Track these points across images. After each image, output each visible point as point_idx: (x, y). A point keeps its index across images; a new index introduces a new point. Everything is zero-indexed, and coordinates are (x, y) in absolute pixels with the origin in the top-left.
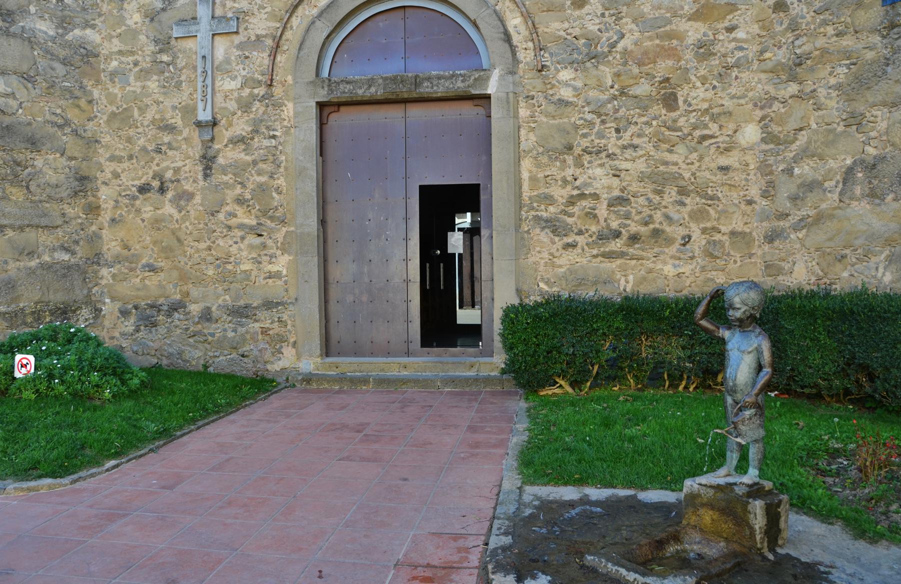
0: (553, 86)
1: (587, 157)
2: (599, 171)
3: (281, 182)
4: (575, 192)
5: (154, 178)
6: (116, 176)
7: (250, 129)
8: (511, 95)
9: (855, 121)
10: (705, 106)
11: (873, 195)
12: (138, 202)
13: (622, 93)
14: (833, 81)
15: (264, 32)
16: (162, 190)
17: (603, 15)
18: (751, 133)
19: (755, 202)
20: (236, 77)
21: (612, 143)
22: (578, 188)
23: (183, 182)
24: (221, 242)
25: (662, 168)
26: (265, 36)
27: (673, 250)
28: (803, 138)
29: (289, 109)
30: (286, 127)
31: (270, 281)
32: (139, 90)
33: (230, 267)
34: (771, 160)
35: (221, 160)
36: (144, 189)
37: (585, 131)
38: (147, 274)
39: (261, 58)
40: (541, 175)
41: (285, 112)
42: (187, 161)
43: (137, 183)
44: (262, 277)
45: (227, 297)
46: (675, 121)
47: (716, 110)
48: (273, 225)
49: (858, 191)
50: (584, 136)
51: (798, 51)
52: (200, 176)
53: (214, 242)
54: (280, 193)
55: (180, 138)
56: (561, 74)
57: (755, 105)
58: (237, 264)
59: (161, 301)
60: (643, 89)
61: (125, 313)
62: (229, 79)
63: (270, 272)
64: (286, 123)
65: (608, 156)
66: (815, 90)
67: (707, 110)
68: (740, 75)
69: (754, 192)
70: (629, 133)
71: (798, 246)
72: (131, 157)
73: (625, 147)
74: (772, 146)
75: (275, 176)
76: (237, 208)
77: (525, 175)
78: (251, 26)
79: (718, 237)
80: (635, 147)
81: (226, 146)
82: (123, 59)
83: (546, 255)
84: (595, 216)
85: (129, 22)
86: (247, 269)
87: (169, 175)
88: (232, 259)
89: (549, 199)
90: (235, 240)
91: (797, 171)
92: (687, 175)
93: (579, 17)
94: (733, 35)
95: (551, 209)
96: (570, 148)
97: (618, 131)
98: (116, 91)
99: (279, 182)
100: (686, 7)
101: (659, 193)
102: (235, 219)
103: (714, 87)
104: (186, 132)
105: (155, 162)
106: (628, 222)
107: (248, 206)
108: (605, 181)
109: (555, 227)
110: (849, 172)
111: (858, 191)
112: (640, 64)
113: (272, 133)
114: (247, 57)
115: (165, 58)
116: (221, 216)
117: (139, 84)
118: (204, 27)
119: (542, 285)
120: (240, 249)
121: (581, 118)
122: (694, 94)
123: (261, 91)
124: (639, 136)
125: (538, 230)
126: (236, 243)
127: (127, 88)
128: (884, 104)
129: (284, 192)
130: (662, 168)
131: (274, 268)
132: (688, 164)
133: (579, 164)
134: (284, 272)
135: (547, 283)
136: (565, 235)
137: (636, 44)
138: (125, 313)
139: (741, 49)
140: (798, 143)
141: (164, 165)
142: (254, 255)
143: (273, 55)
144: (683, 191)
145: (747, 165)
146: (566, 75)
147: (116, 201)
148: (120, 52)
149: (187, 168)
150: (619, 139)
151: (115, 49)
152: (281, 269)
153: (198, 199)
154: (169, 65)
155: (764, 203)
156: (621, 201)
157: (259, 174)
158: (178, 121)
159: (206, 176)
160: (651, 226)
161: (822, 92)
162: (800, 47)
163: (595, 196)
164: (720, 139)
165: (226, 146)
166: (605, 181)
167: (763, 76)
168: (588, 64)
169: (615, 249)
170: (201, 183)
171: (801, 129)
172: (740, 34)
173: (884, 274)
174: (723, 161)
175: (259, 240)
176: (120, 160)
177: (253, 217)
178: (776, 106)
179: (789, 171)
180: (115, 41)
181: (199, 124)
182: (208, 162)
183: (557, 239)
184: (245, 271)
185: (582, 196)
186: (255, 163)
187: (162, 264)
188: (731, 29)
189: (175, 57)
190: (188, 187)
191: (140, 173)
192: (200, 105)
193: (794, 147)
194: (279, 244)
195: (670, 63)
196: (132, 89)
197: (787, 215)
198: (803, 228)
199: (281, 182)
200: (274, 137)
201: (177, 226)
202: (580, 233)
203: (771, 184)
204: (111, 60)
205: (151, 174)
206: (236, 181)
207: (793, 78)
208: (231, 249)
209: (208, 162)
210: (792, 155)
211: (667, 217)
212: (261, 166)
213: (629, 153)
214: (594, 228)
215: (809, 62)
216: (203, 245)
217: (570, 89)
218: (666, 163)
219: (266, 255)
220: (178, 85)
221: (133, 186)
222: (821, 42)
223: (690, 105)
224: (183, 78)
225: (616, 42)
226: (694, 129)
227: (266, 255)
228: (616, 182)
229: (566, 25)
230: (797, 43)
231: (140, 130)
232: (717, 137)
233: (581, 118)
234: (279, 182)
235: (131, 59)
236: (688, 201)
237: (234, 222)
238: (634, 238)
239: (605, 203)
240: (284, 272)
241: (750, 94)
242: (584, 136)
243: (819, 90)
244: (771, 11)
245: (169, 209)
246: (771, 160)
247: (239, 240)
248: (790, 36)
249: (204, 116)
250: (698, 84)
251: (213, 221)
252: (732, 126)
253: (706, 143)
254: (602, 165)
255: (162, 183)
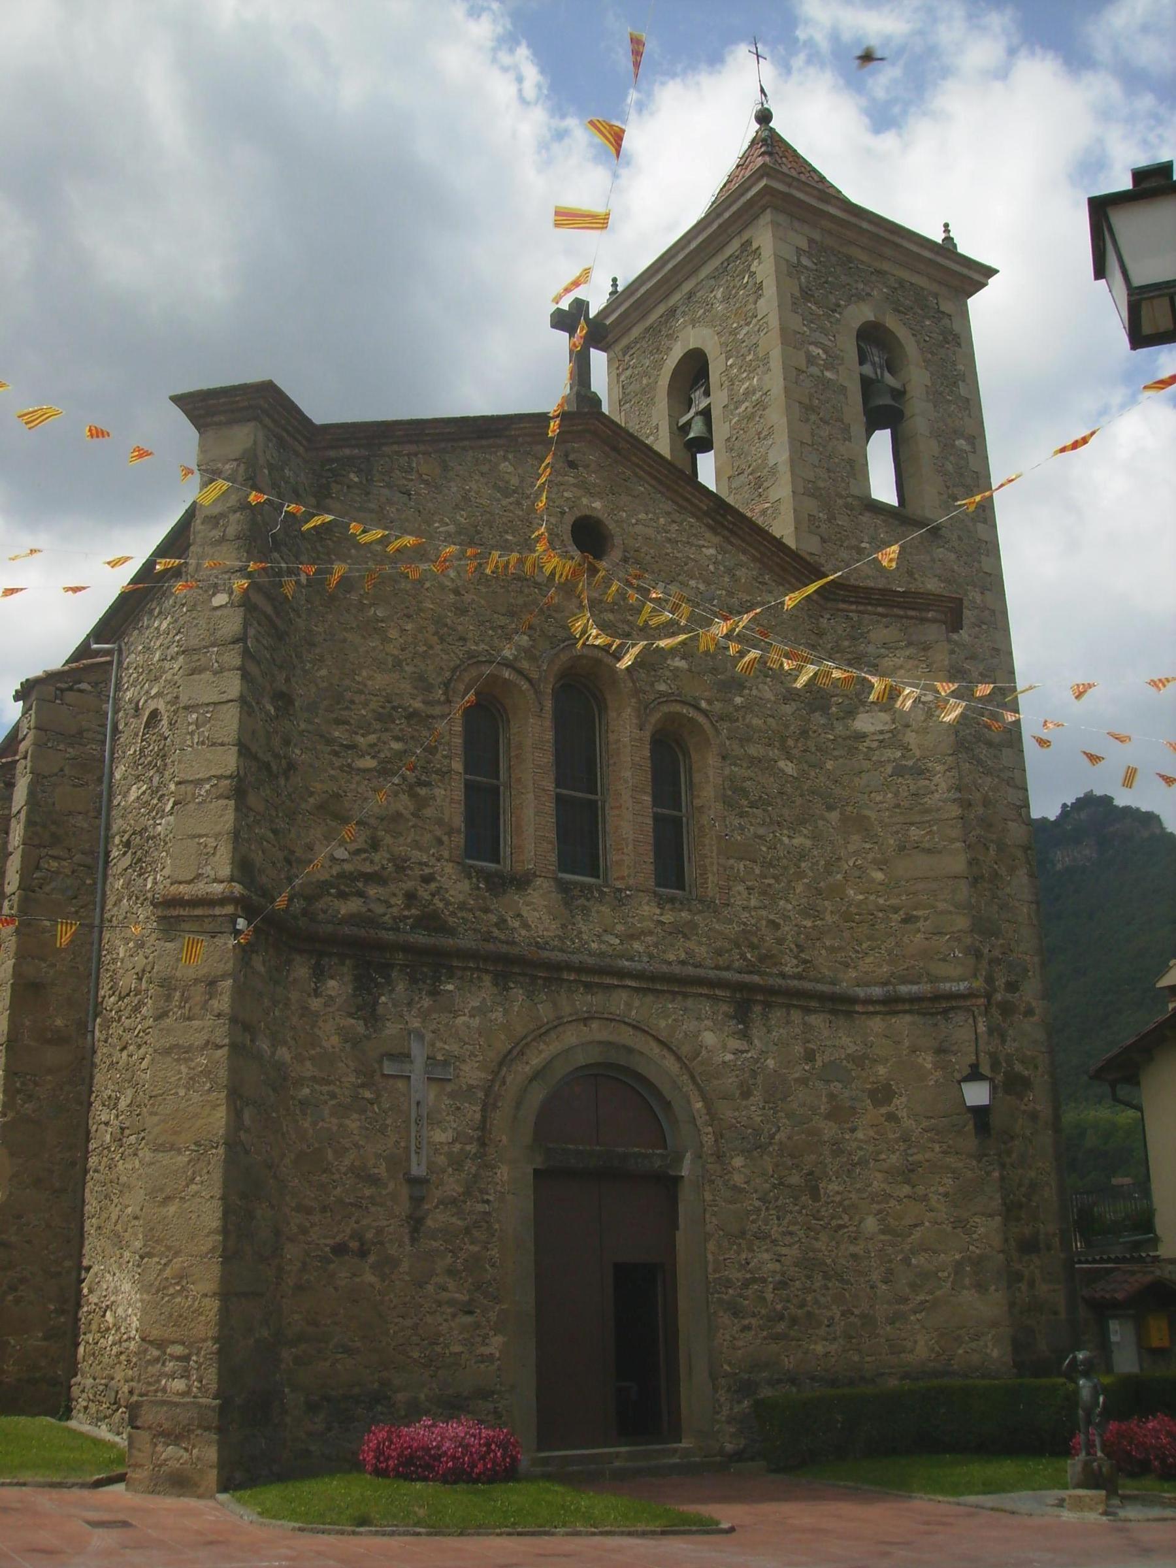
0: (730, 1172)
1: (757, 1242)
2: (766, 1256)
3: (494, 1252)
4: (748, 1276)
5: (351, 1237)
6: (304, 1231)
7: (461, 1190)
8: (700, 1179)
9: (960, 1224)
10: (838, 1198)
11: (981, 1287)
12: (332, 1266)
13: (781, 1184)
14: (941, 1190)
15: (475, 1083)
16: (363, 1254)
17: (764, 1108)
18: (871, 1224)
19: (876, 1287)
20: (446, 1129)
21: (775, 1232)
22: (751, 1272)
23: (387, 1245)
24: (429, 1319)
25: (811, 1254)
26: (476, 1087)
27: (822, 1331)
28: (917, 1234)
29: (503, 1172)
30: (500, 1192)
31: (482, 1366)
32: (335, 1128)
33: (438, 1349)
34: (890, 1250)
35: (429, 1223)
36: (340, 1250)
37: (754, 1217)
38: (340, 1356)
39: (473, 1112)
40: (721, 1258)
41: (499, 1174)
42: (392, 1221)
43: (330, 1242)
44: (473, 1362)
45: (434, 1386)
46: (818, 1211)
47: (846, 1203)
48: (485, 1302)
49: (967, 1281)
50: (753, 1222)
51: (910, 1159)
52: (406, 1240)
53: (421, 1320)
54: (493, 1266)
55: (384, 1192)
56: (734, 1160)
57: (873, 1199)
58: (447, 1346)
59: (356, 1390)
60: (795, 1179)
61: (312, 1408)
62: (438, 1130)
63: (482, 1355)
64: (499, 1188)
65: (772, 1242)
66: (926, 1195)
67: (840, 1203)
68: (862, 1172)
69: (875, 1276)
70: (786, 1221)
71: (917, 1326)
72: (324, 1209)
73: (784, 1234)
74: (887, 1237)
75: (489, 1246)
76: (448, 1280)
77: (710, 1257)
78: (462, 1073)
79: (852, 1319)
80: (791, 1233)
81: (437, 1207)
82: (317, 1087)
83: (728, 1337)
84: (764, 1299)
85: (324, 1043)
86: (457, 1351)
87: (369, 1235)
88: (442, 1339)
89: (728, 1284)
90: (445, 1316)
91: (914, 1261)
92: (829, 1261)
93: (746, 1107)
94: (855, 1135)
95: (731, 1291)
96: (743, 1233)
97: (778, 1218)
98: (306, 1125)
99: (493, 1253)
100: (822, 1107)
101: (809, 1277)
102: (444, 1293)
103: (845, 1182)
104: (391, 1186)
105: (354, 1219)
106: (788, 1305)
107: (461, 1278)
108: (772, 1266)
109: (736, 1312)
110: (958, 1267)
111: (967, 1281)
112: (792, 1156)
113: (486, 1197)
114: (458, 1108)
115: (368, 1094)
116: (430, 1288)
117: (335, 1121)
118: (417, 1069)
119: (726, 1367)
120: (451, 1329)
121: (750, 1205)
122: (830, 1187)
123: (472, 1148)
124: (795, 1224)
125: (721, 1314)
126: (446, 1320)
127: (321, 1124)
128: (983, 1214)
129: (498, 1264)
130: (811, 1254)
131: (486, 1350)
132: (830, 1251)
133: (751, 1250)
134: (497, 1355)
135: (730, 1364)
136: (743, 1318)
137: (789, 1138)
138: (312, 1408)
139: (861, 1149)
140: (913, 1237)
141: (364, 1222)
142: (466, 1336)
143: (487, 1108)
144: (826, 1276)
145: (869, 1252)
146: (738, 1162)
147: (304, 1263)
148: (313, 1078)
149: (391, 1229)
150: (779, 1226)
151: (308, 1074)
152: (493, 1352)
153: (405, 1266)
154: (372, 1104)
155: (884, 1287)
156: (783, 1285)
157: (472, 1243)
158: (382, 1170)
159: (413, 1240)
160: (806, 1309)
161: (934, 1198)
162: (912, 1155)
163: (764, 1280)
164: (851, 1229)
165: (437, 1207)
166: (772, 1266)
167: (878, 1175)
168: (755, 1153)
169: (780, 1330)
170: (408, 1248)
171: (916, 1226)
172: (860, 1135)
173: (992, 1350)
174: (853, 1249)
175: (469, 1319)
176: (309, 1211)
177: (465, 1292)
178: (892, 1203)
179: (906, 1261)
180: (308, 1064)
181: (413, 1181)
182: (416, 1223)
183: (736, 1321)
184: (456, 1354)
185: (754, 1280)
186: (467, 1231)
187: (359, 1344)
188: (853, 1130)
189: (379, 1096)
190: (393, 1250)
191: (335, 1230)
192: (414, 1158)
193: (909, 1240)
194: (492, 1323)
195: (813, 1157)
196: (326, 1125)
197: (907, 1299)
198: (921, 1311)
199: (494, 1252)
200: (487, 1202)
201: (378, 1298)
202: (754, 1315)
203: (890, 1272)
204: (303, 1085)
205: (348, 1231)
206: (446, 1248)
207: (908, 1182)
208: (441, 1328)
209: (416, 1223)
210: (908, 1247)
211: (816, 1302)
212: (476, 1233)
213: (788, 1240)
214: (763, 1312)
215: (920, 1169)
216: (409, 1322)
217: (742, 1176)
218: (814, 1251)
219: (479, 1335)
220: (383, 1131)
221: (326, 1245)
222: (928, 1155)
223: (829, 1197)
224: (389, 1121)
225: (775, 1134)
226: (832, 1219)
227: (479, 1335)
228: (778, 1266)
229: (736, 1114)
230: (909, 1152)
231: (336, 1177)
232: (847, 1227)
233: (750, 1205)
234: (493, 1253)
235: (325, 1089)
236: (830, 1285)
237: (445, 1295)
238: (794, 1321)
239: (771, 1286)
240: (497, 1355)
241: (869, 1189)
242: (753, 1222)
243: (930, 1195)
244: (883, 1119)
245: (369, 1278)
246: (890, 1250)
247: (449, 1317)
248: (903, 1146)
249: (417, 1170)
250: (834, 1178)
251: (421, 1294)
252: (857, 1218)
253: (840, 1233)
254: (767, 1251)
255: (362, 1245)
